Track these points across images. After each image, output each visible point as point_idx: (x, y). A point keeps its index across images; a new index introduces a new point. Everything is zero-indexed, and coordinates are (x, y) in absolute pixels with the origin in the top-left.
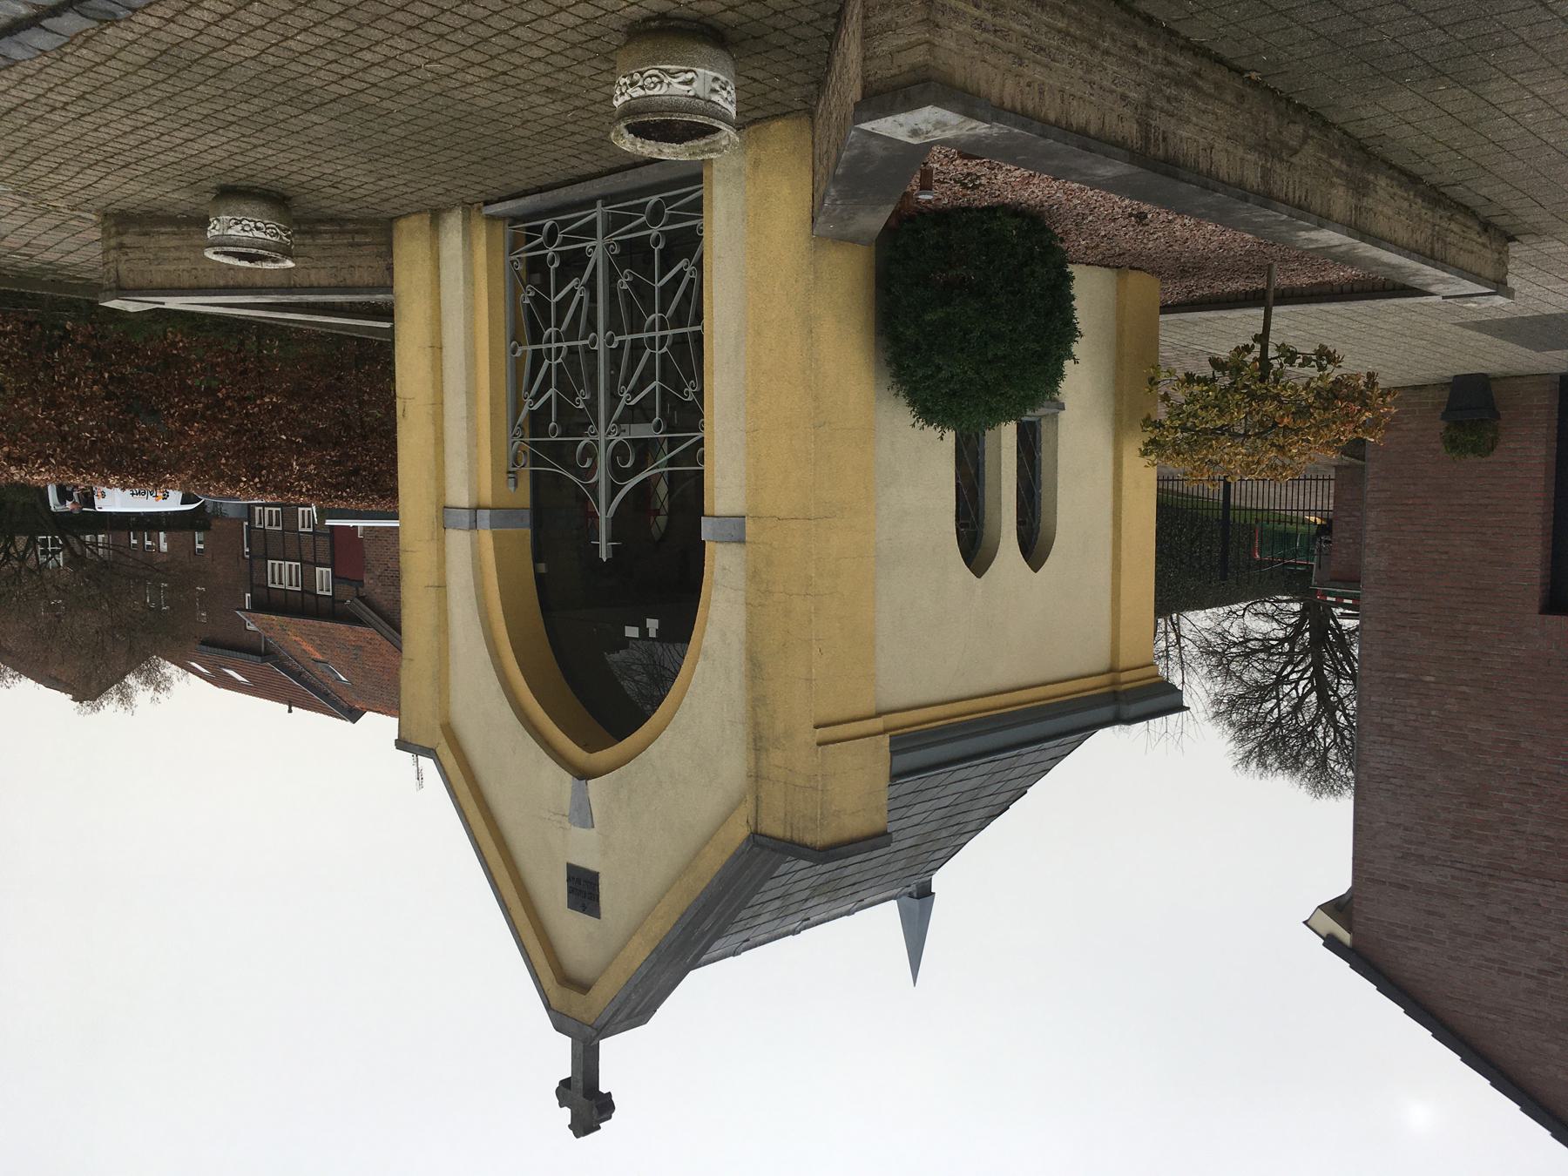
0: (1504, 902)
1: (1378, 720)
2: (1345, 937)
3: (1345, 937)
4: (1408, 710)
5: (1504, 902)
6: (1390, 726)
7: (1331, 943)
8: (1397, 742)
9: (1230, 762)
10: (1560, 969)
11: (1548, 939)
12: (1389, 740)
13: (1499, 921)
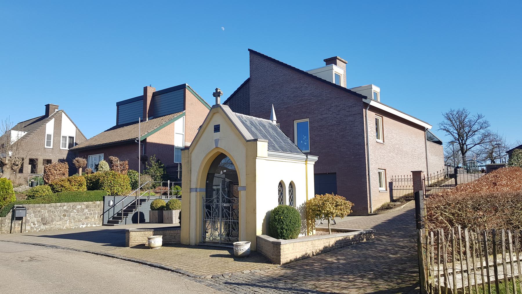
0: (337, 118)
1: (361, 147)
2: (364, 100)
3: (364, 100)
4: (356, 150)
5: (337, 118)
6: (359, 146)
7: (366, 98)
8: (357, 143)
10: (328, 110)
11: (331, 114)
12: (359, 143)
13: (338, 114)
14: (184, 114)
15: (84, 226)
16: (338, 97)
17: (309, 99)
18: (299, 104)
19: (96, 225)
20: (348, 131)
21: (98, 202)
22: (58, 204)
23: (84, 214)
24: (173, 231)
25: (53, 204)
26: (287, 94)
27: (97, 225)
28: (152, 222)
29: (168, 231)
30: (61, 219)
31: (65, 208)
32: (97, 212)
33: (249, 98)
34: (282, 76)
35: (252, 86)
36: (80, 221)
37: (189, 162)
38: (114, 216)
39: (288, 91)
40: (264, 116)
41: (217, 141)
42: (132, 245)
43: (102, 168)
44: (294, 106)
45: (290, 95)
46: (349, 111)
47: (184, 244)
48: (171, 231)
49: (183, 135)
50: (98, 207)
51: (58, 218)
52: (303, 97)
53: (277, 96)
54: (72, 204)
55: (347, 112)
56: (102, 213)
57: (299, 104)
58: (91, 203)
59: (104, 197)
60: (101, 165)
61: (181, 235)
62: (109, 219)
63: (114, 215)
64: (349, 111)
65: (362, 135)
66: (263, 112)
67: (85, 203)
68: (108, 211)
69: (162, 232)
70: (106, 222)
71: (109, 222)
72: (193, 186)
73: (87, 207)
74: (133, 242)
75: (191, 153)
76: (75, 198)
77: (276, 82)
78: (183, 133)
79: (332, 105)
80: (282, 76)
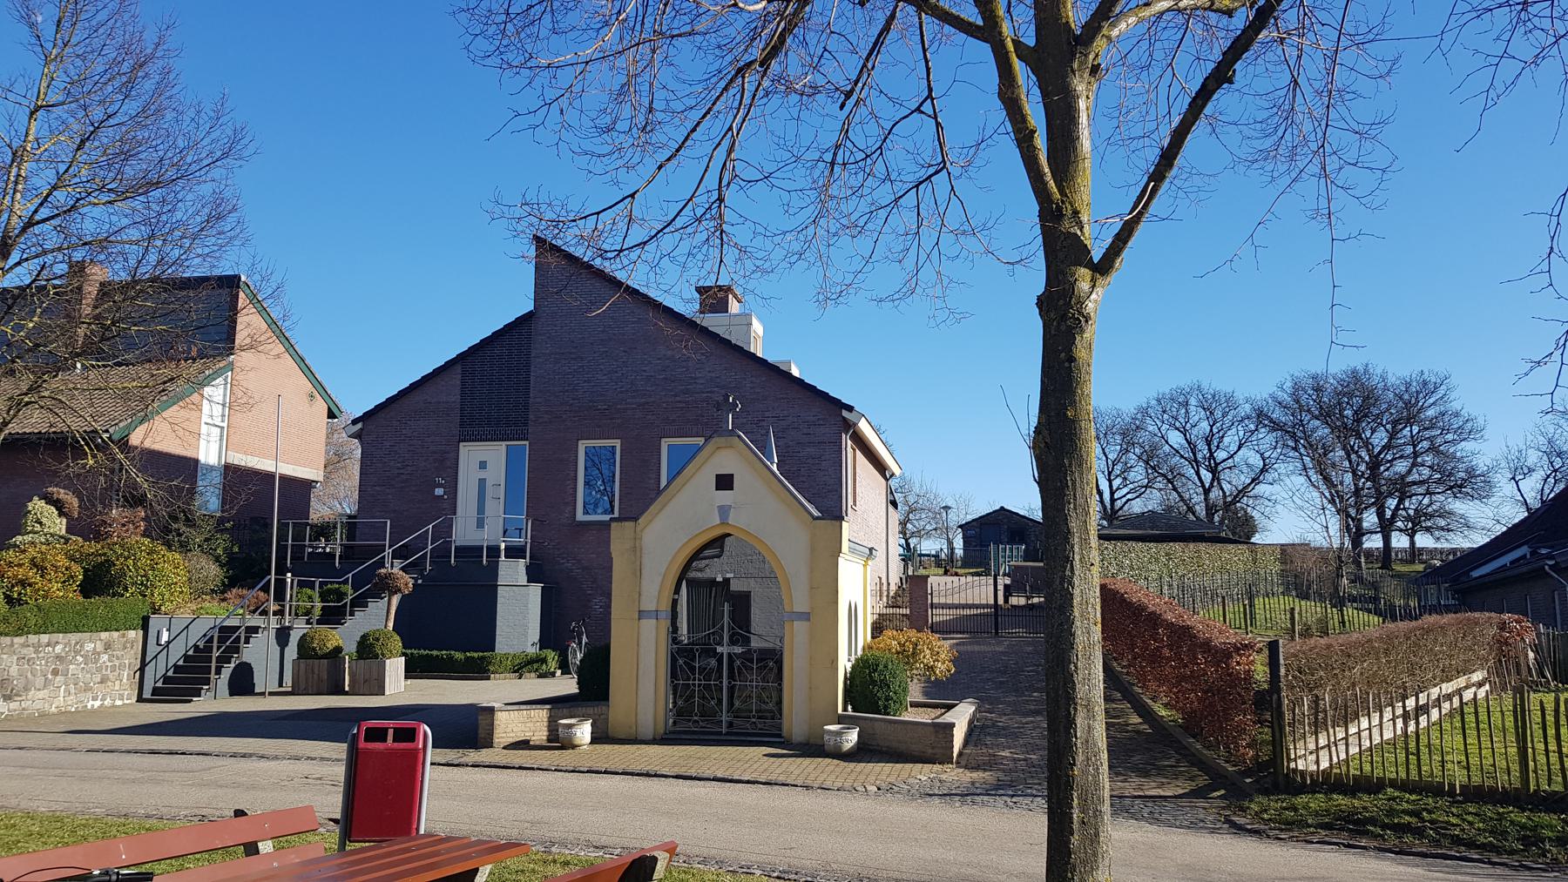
2: (845, 413)
3: (845, 413)
7: (850, 409)
9: (1453, 381)
14: (231, 367)
15: (97, 704)
16: (783, 398)
17: (708, 392)
18: (678, 399)
19: (123, 700)
20: (805, 480)
21: (132, 634)
22: (45, 638)
23: (99, 670)
24: (592, 709)
25: (33, 638)
26: (645, 371)
27: (126, 702)
28: (304, 692)
29: (580, 709)
30: (47, 683)
31: (58, 648)
32: (127, 662)
33: (528, 365)
34: (633, 323)
35: (540, 334)
36: (87, 689)
37: (636, 550)
38: (166, 673)
39: (650, 362)
40: (574, 417)
41: (724, 511)
42: (499, 742)
43: (41, 523)
44: (664, 403)
45: (653, 374)
46: (807, 434)
47: (620, 737)
48: (588, 708)
49: (222, 428)
50: (132, 648)
51: (40, 681)
52: (691, 384)
53: (616, 372)
54: (74, 637)
55: (804, 434)
56: (147, 668)
57: (678, 399)
58: (115, 634)
59: (146, 620)
60: (36, 514)
61: (610, 719)
62: (155, 683)
63: (167, 671)
64: (807, 434)
65: (837, 491)
66: (571, 405)
67: (104, 635)
68: (155, 660)
69: (568, 710)
70: (147, 694)
71: (155, 691)
72: (649, 604)
73: (108, 646)
74: (503, 735)
75: (642, 531)
76: (53, 621)
77: (614, 334)
78: (222, 424)
79: (767, 414)
80: (633, 323)
